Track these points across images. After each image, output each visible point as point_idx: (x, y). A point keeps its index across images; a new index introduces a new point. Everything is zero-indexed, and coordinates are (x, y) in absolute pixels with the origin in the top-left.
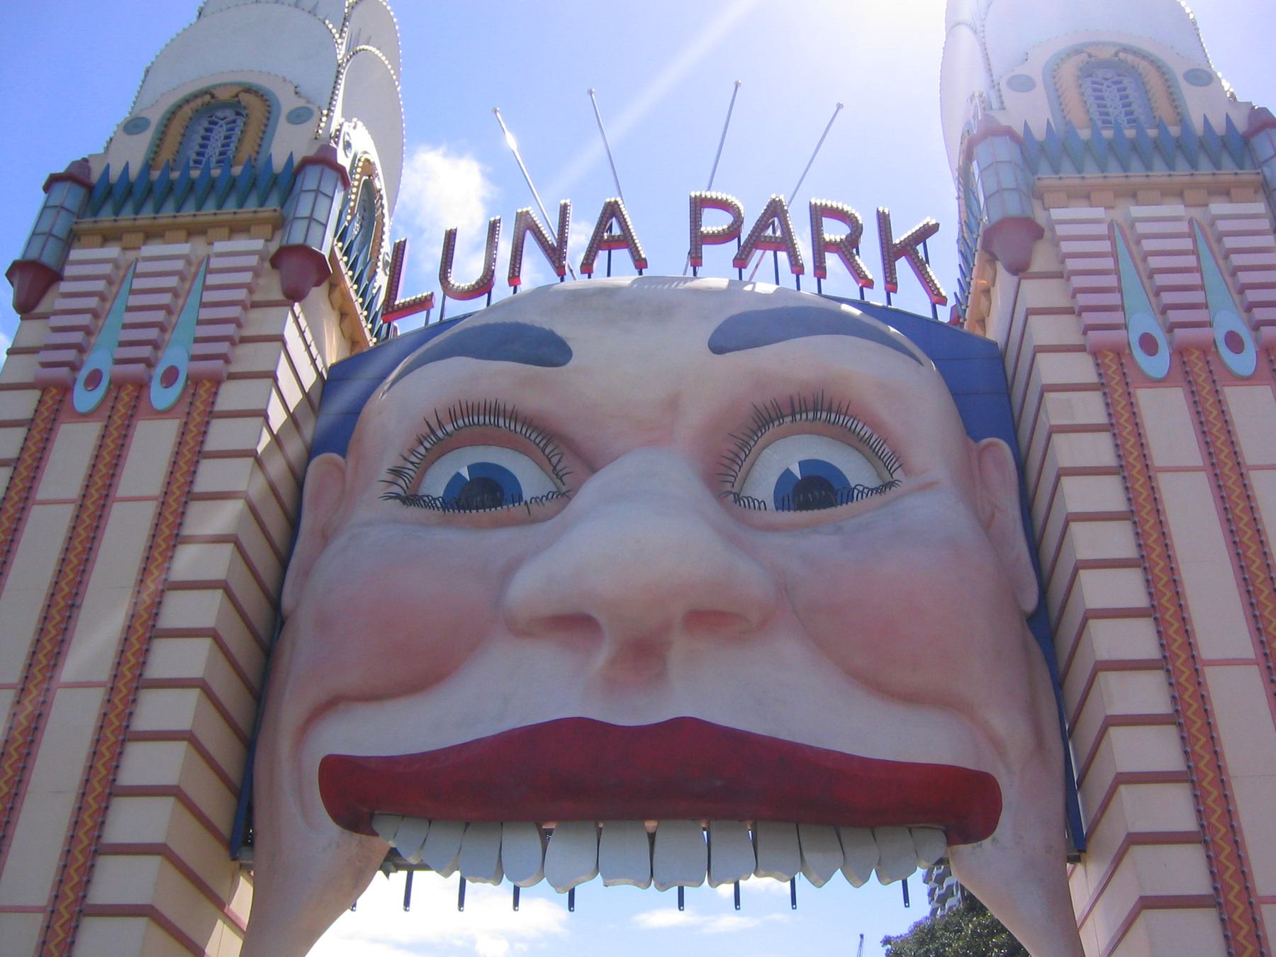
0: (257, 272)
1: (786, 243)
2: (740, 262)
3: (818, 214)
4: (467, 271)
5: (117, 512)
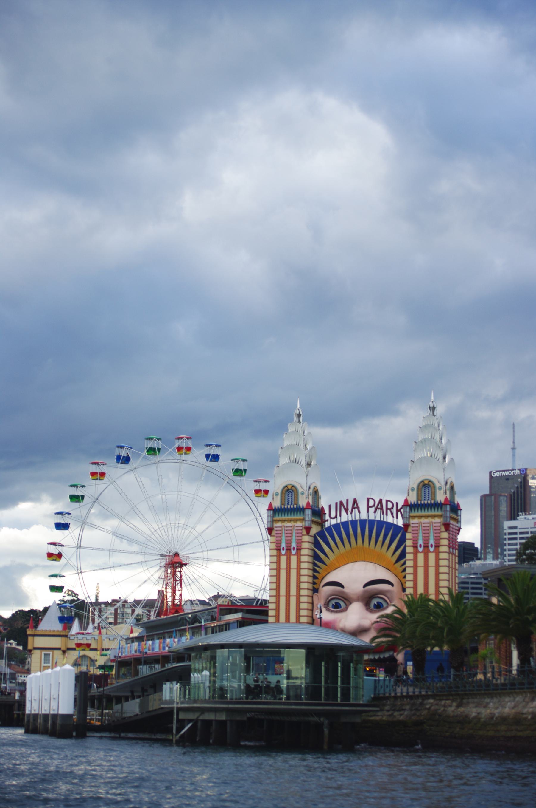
0: (301, 530)
1: (382, 509)
2: (375, 512)
3: (387, 501)
4: (333, 514)
5: (292, 571)
